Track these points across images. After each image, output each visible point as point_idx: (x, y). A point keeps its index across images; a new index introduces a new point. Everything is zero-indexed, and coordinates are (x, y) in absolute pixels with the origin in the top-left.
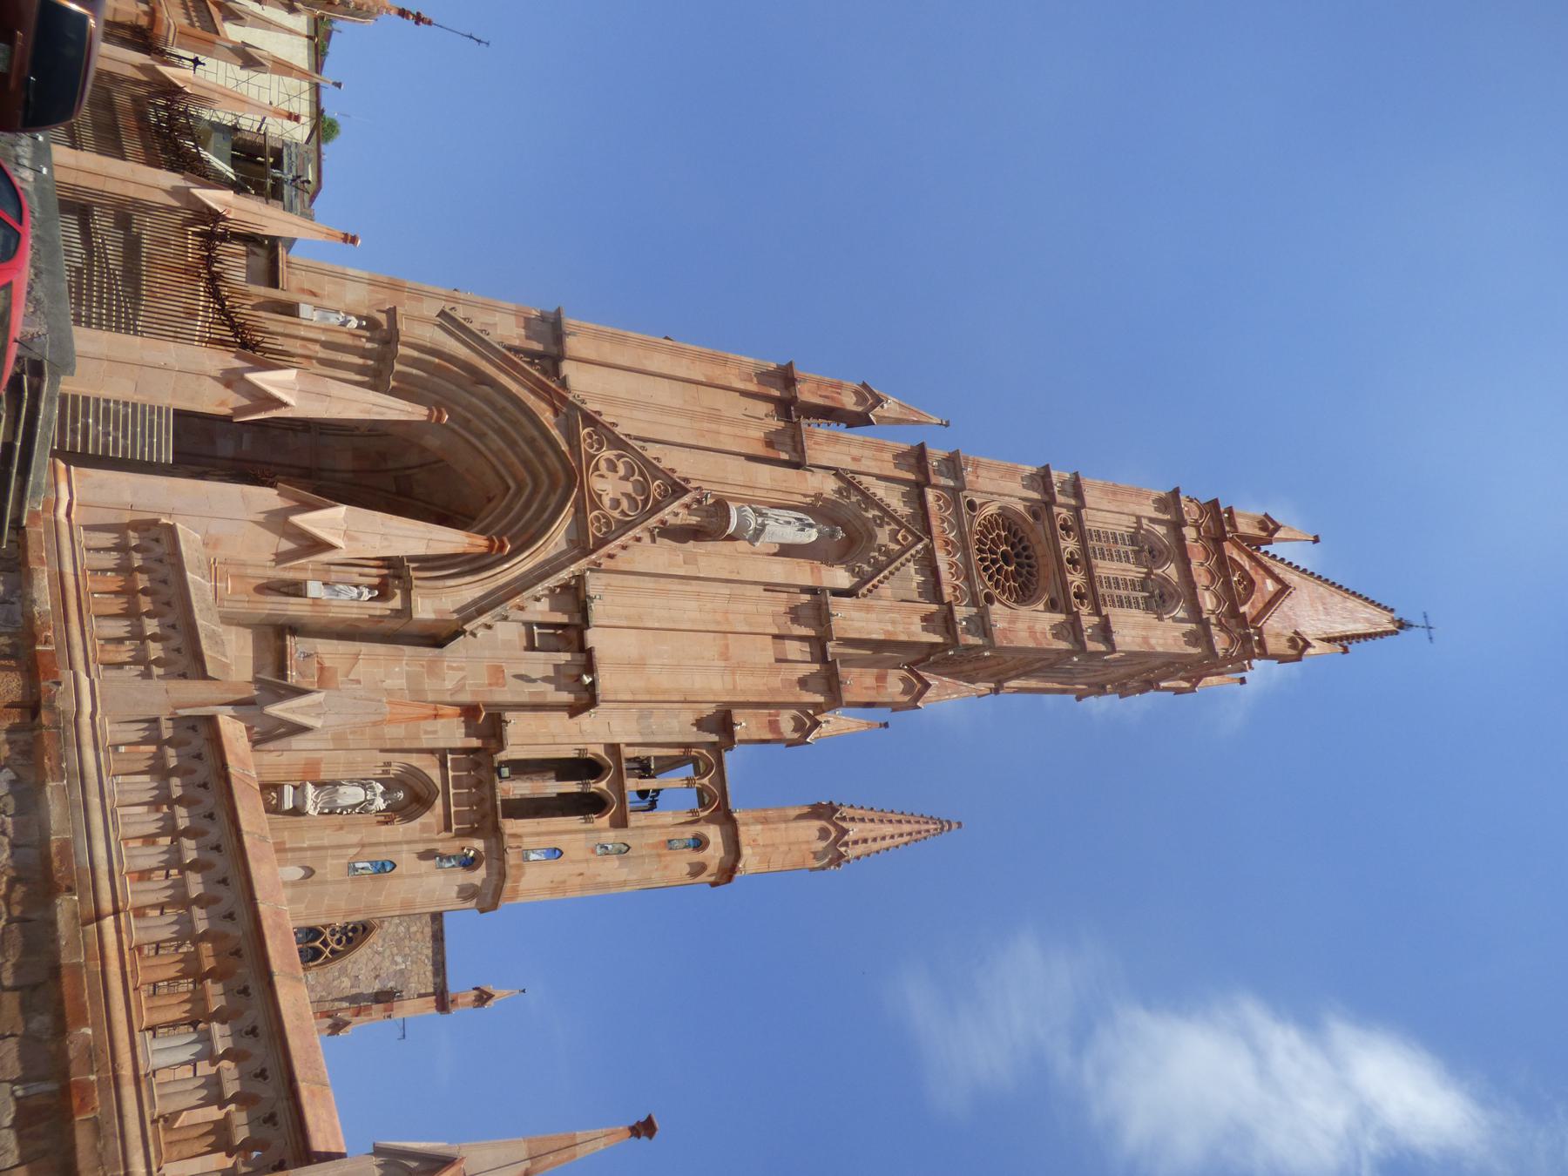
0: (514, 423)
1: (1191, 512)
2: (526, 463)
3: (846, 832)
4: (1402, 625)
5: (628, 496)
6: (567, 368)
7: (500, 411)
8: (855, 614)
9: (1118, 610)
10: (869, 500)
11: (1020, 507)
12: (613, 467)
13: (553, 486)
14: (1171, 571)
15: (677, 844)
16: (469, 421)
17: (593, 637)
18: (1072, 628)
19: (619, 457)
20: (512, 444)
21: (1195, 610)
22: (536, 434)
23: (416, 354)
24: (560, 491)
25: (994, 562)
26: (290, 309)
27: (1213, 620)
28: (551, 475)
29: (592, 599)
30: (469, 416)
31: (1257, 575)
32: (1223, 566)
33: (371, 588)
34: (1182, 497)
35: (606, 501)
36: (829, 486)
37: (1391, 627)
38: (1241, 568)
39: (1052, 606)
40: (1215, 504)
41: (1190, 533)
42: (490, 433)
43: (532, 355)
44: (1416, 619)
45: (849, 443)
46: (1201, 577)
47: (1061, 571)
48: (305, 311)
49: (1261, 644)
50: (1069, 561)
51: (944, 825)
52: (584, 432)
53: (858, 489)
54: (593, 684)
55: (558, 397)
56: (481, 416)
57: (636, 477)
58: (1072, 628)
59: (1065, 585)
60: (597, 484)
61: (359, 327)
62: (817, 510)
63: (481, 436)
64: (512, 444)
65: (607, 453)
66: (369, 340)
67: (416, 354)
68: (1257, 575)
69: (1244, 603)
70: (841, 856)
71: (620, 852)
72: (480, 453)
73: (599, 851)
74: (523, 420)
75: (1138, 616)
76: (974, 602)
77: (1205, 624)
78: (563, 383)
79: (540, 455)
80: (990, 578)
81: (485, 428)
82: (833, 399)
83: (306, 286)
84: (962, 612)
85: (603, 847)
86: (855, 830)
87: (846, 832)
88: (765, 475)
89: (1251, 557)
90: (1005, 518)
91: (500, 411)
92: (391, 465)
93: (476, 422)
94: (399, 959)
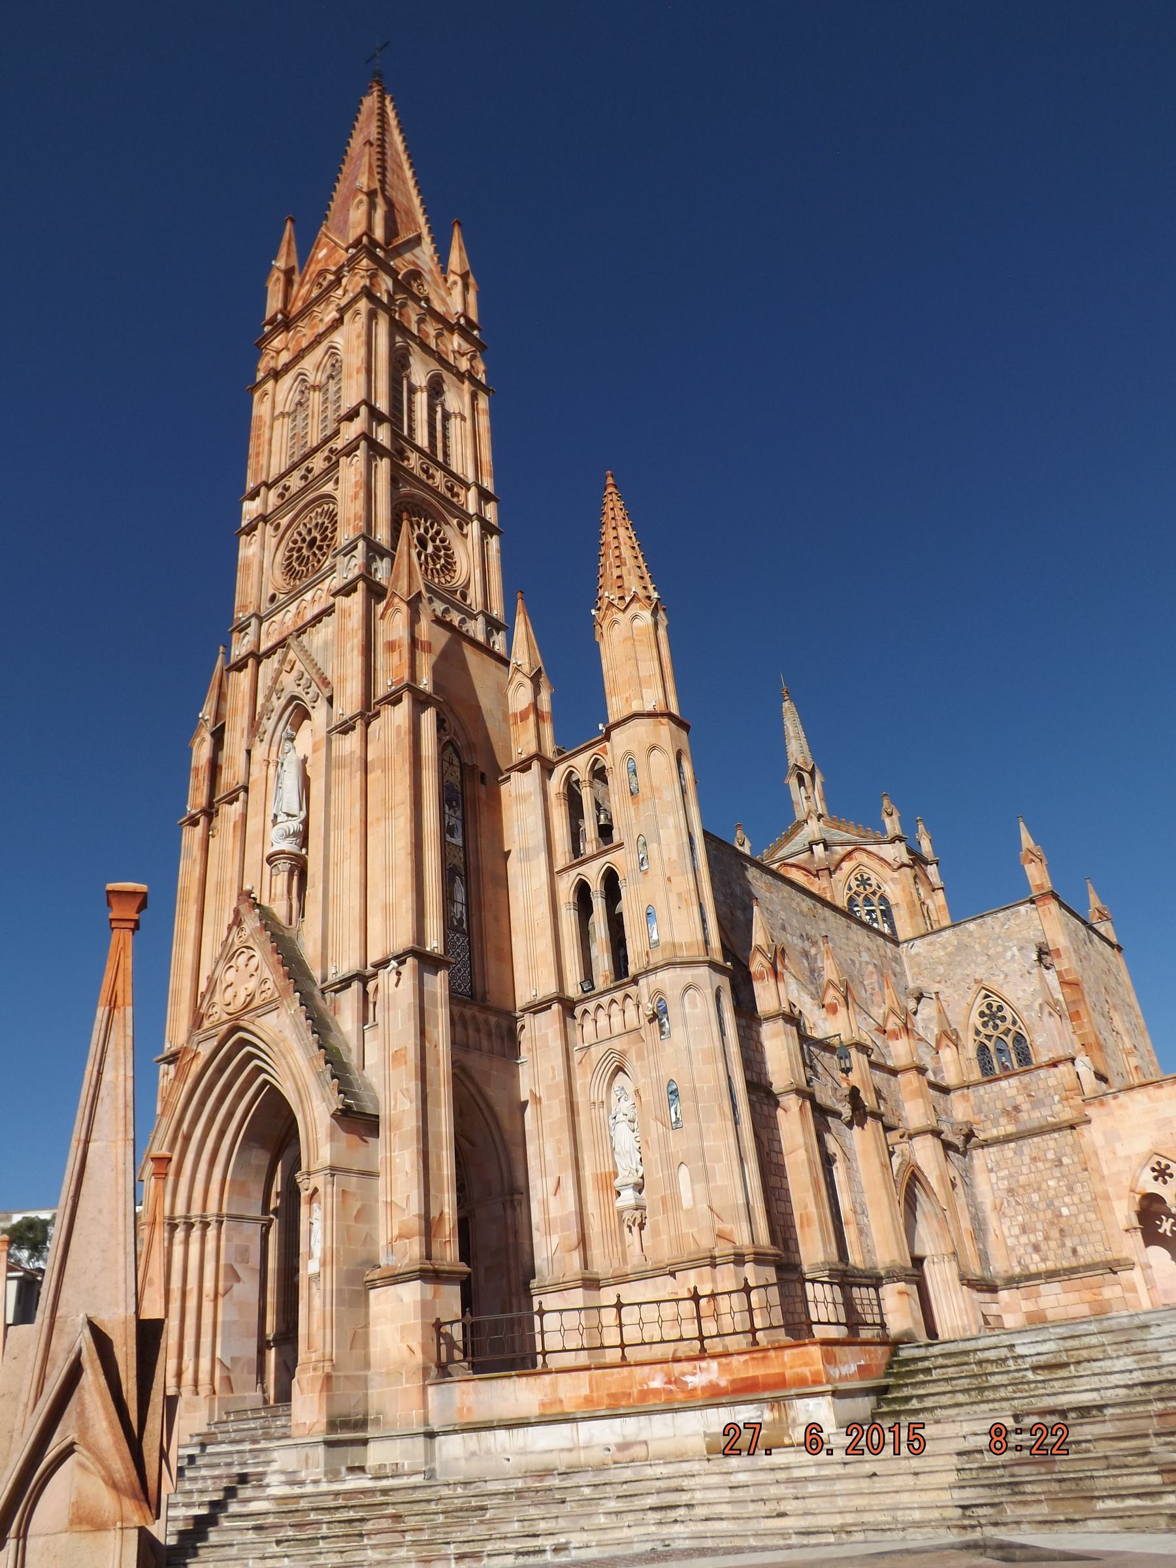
25: (314, 554)
35: (252, 985)
54: (395, 958)
94: (1009, 954)
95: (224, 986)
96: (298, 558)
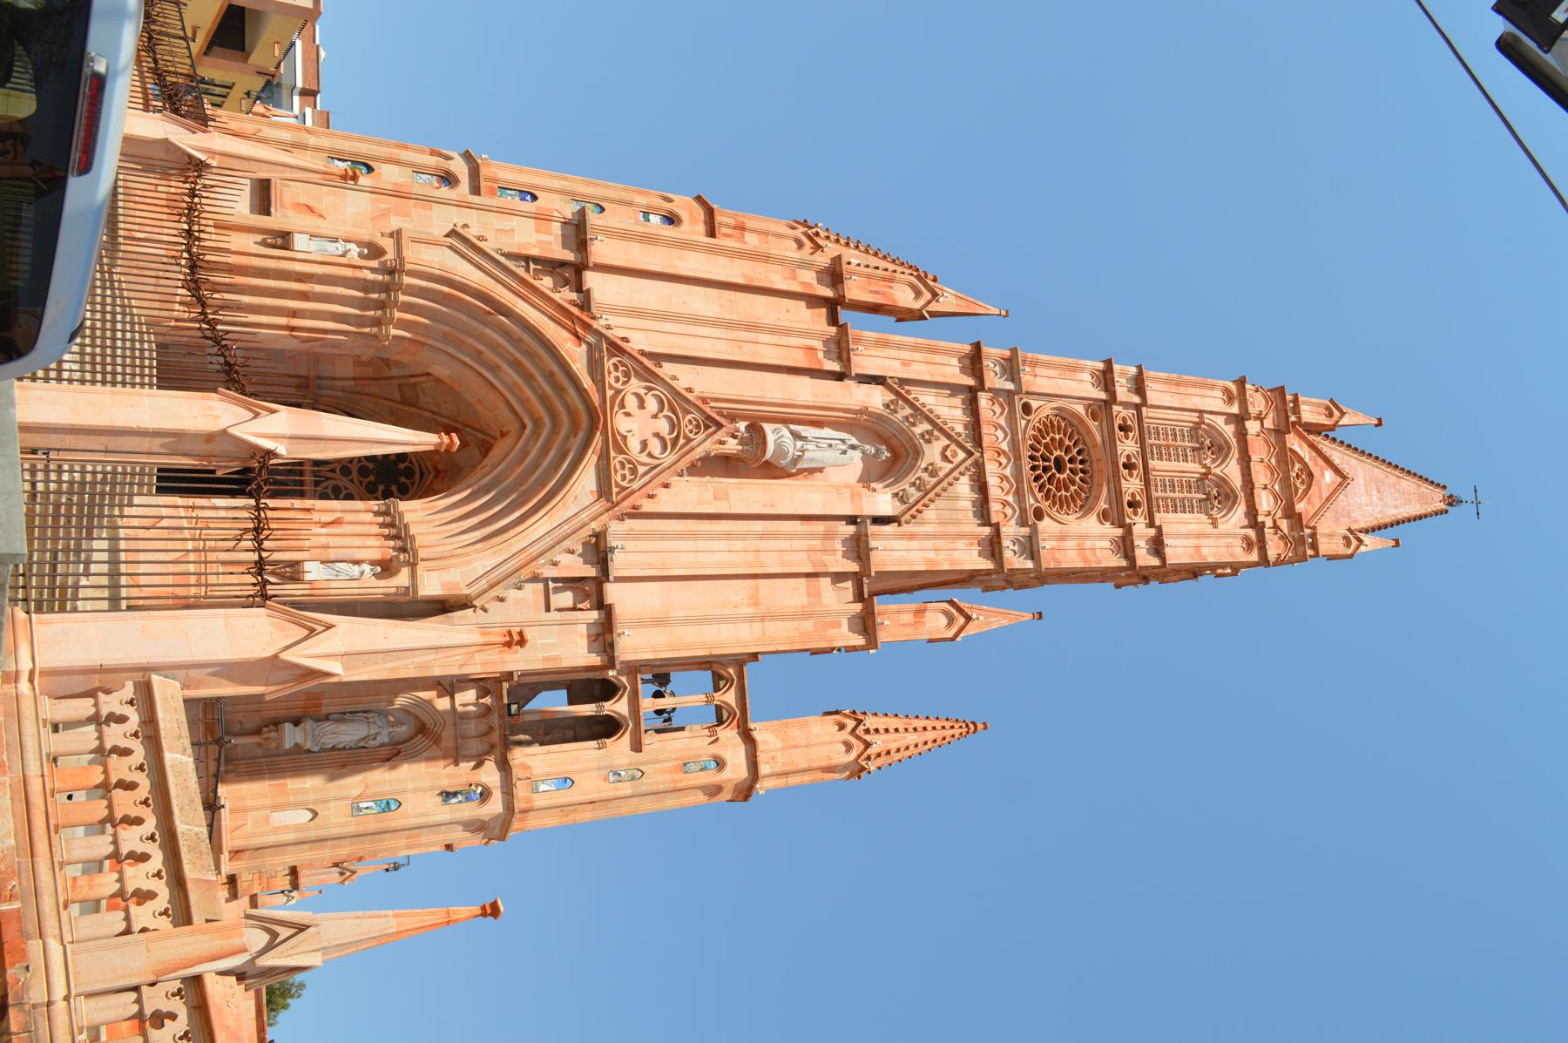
0: (532, 356)
1: (1257, 403)
2: (543, 398)
3: (868, 745)
4: (1452, 501)
5: (657, 435)
6: (591, 279)
7: (517, 342)
8: (898, 544)
9: (1171, 515)
10: (919, 413)
11: (1080, 409)
12: (642, 405)
13: (574, 429)
14: (1232, 470)
15: (692, 766)
16: (480, 353)
17: (614, 593)
18: (1125, 546)
19: (650, 389)
20: (528, 377)
21: (1252, 512)
22: (555, 368)
23: (423, 283)
24: (581, 435)
25: (1046, 469)
26: (283, 239)
27: (1269, 523)
28: (572, 413)
29: (612, 550)
30: (482, 348)
31: (1315, 465)
32: (1285, 457)
33: (373, 563)
34: (1248, 386)
35: (634, 445)
36: (876, 398)
37: (1442, 506)
38: (1301, 460)
39: (1104, 516)
40: (1281, 391)
41: (1252, 427)
42: (505, 366)
43: (551, 266)
44: (1466, 495)
45: (899, 346)
46: (1260, 476)
47: (1116, 479)
48: (300, 242)
49: (1314, 546)
50: (1125, 466)
51: (971, 727)
52: (609, 364)
53: (907, 401)
55: (580, 316)
56: (494, 347)
57: (666, 412)
58: (1125, 546)
59: (1119, 492)
60: (622, 424)
61: (361, 255)
62: (862, 425)
63: (494, 369)
64: (528, 377)
65: (635, 385)
66: (373, 270)
67: (423, 283)
68: (1315, 465)
69: (1301, 499)
70: (863, 769)
71: (633, 778)
72: (492, 385)
73: (611, 778)
74: (542, 353)
75: (1195, 522)
76: (1023, 522)
77: (1258, 527)
78: (585, 304)
79: (560, 390)
80: (1041, 488)
81: (499, 361)
82: (884, 294)
83: (303, 200)
84: (1011, 531)
85: (616, 773)
86: (879, 743)
87: (868, 745)
88: (806, 391)
89: (1312, 446)
90: (1065, 422)
91: (517, 342)
92: (395, 372)
93: (488, 354)
95: (642, 392)
96: (1053, 439)
